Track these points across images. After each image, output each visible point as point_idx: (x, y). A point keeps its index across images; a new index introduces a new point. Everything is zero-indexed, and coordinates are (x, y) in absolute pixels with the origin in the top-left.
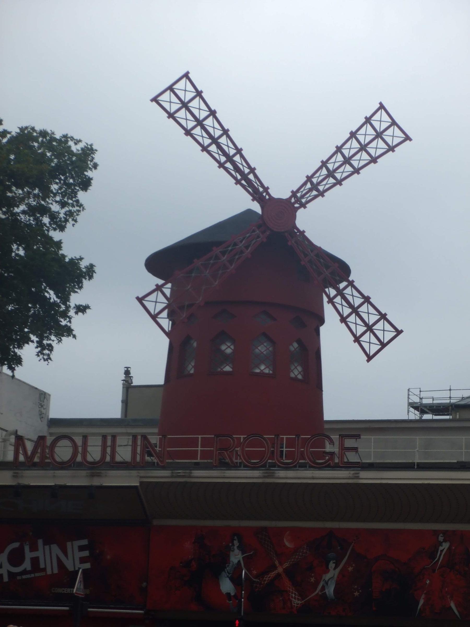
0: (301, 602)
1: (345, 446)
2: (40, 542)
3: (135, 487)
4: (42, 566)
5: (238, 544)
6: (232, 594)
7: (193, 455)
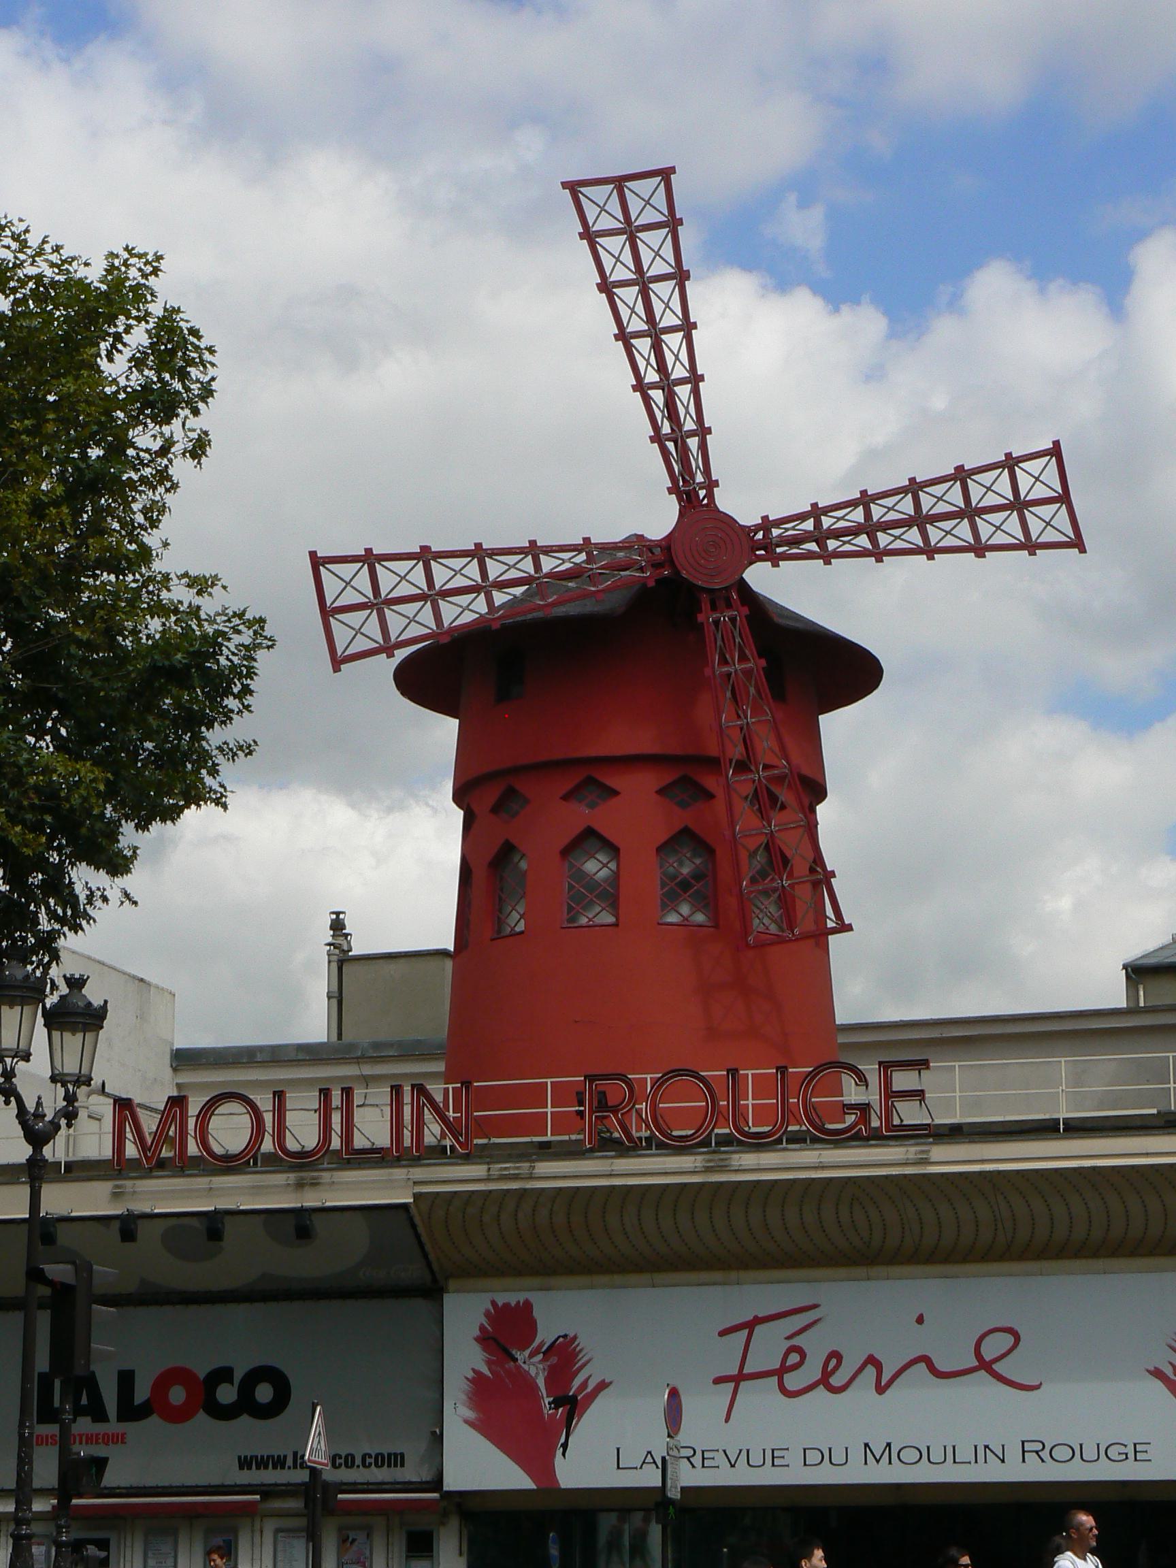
1: (894, 1089)
7: (537, 1124)
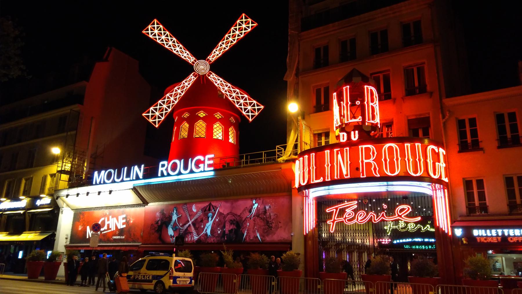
0: (197, 238)
2: (110, 217)
3: (132, 189)
4: (110, 227)
5: (176, 212)
6: (172, 235)
